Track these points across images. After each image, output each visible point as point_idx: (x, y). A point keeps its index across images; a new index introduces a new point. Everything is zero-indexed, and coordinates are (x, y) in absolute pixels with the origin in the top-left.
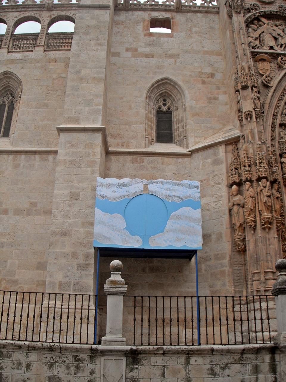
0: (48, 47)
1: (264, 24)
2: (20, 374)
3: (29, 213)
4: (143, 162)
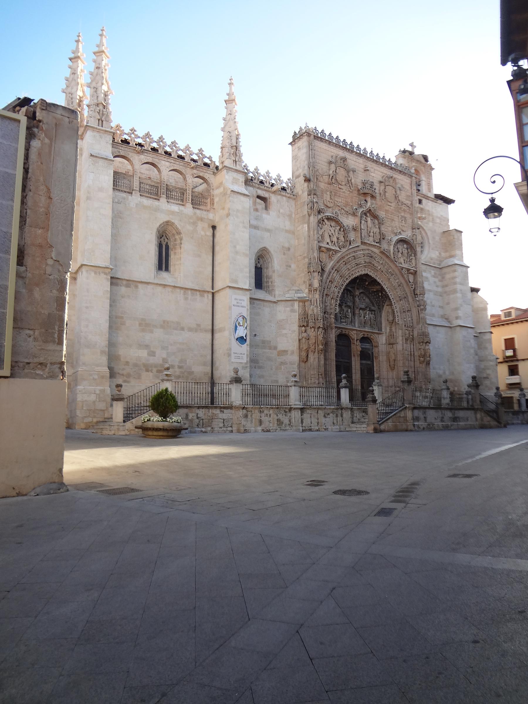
2: (267, 419)
3: (196, 331)
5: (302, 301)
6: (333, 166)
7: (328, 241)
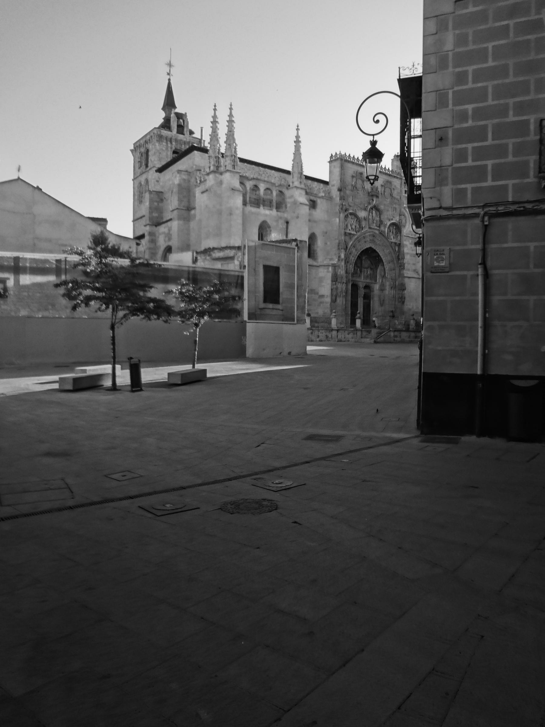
5: (334, 266)
6: (354, 179)
7: (350, 228)
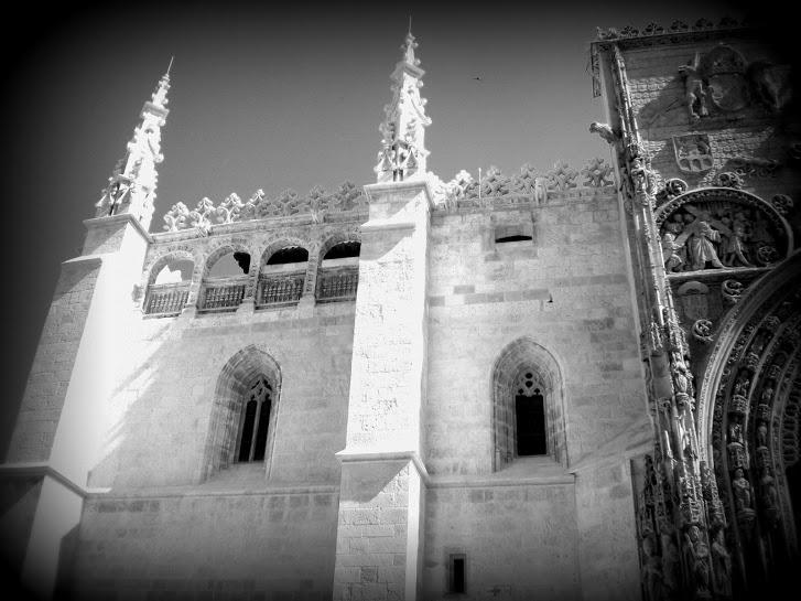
0: (323, 295)
1: (695, 218)
4: (492, 498)
